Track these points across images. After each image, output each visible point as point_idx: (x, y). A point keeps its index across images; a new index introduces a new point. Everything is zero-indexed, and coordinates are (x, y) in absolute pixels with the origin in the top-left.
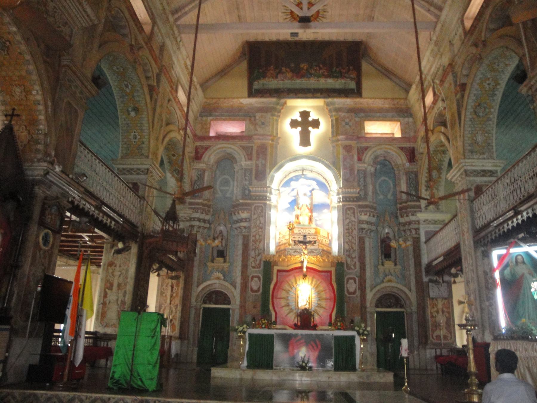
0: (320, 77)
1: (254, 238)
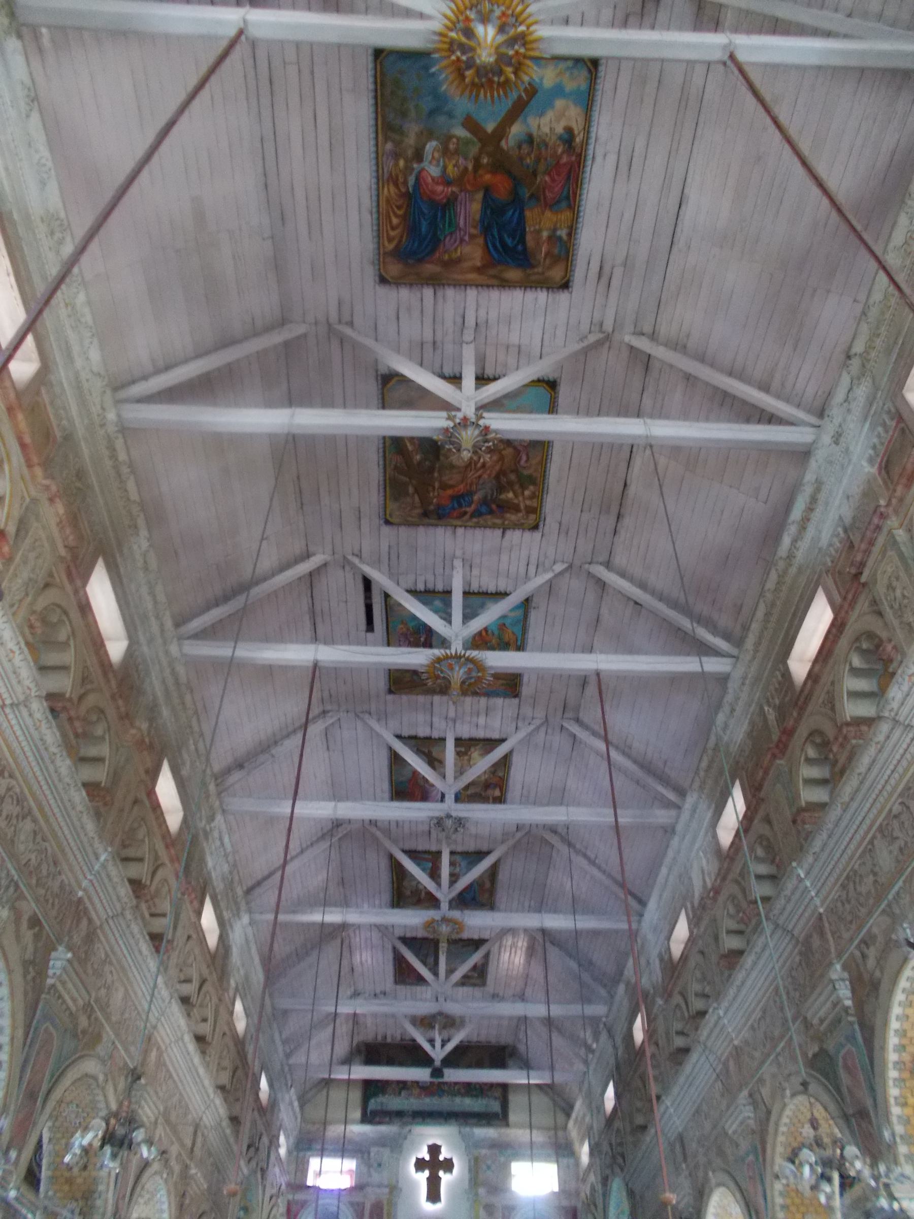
0: (455, 1096)
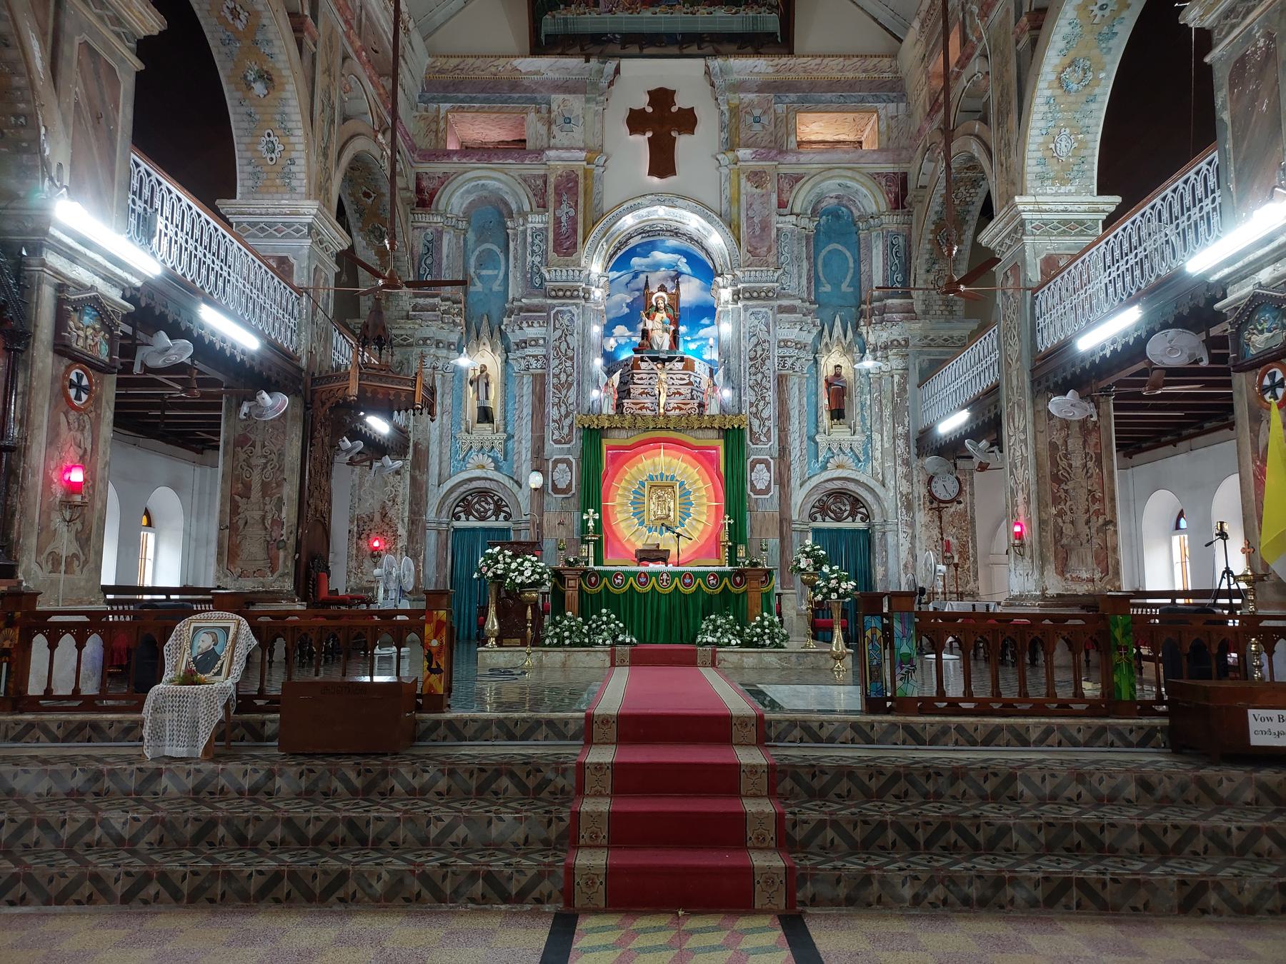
1: (556, 380)
